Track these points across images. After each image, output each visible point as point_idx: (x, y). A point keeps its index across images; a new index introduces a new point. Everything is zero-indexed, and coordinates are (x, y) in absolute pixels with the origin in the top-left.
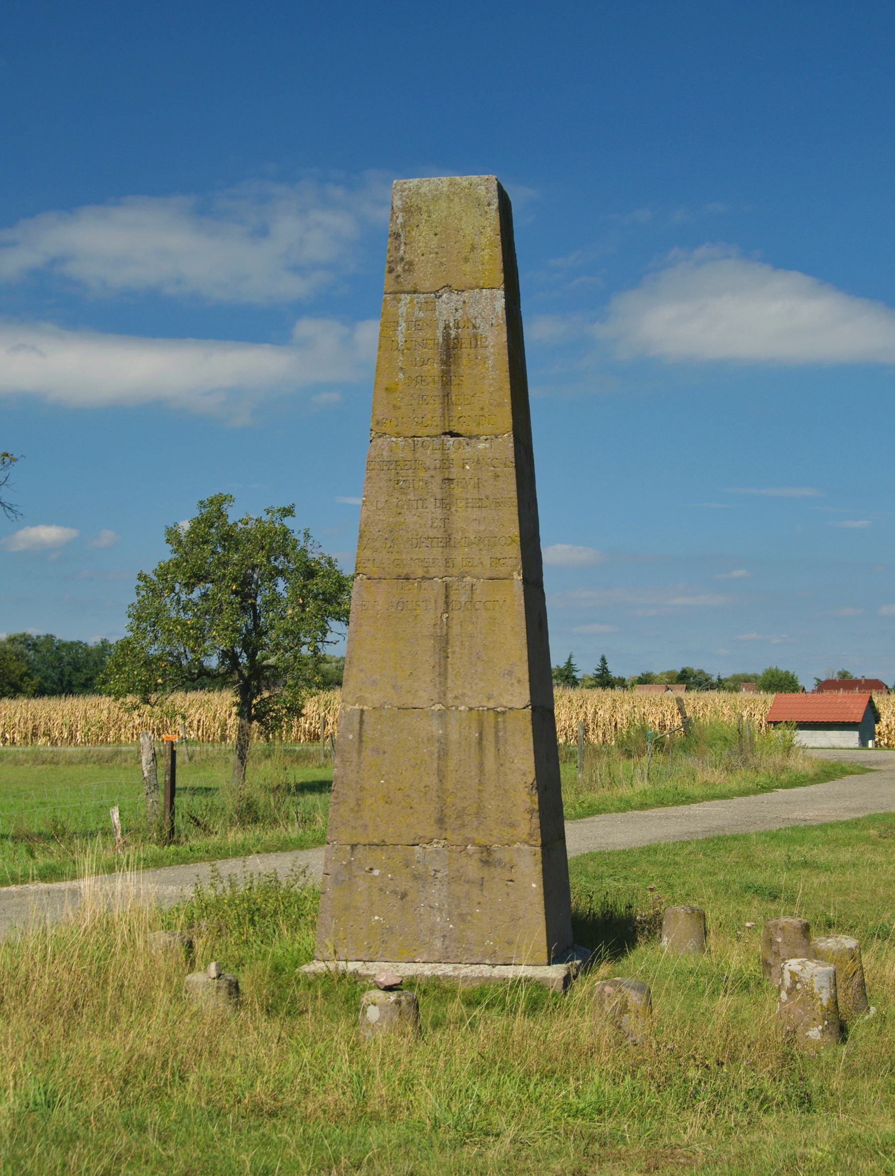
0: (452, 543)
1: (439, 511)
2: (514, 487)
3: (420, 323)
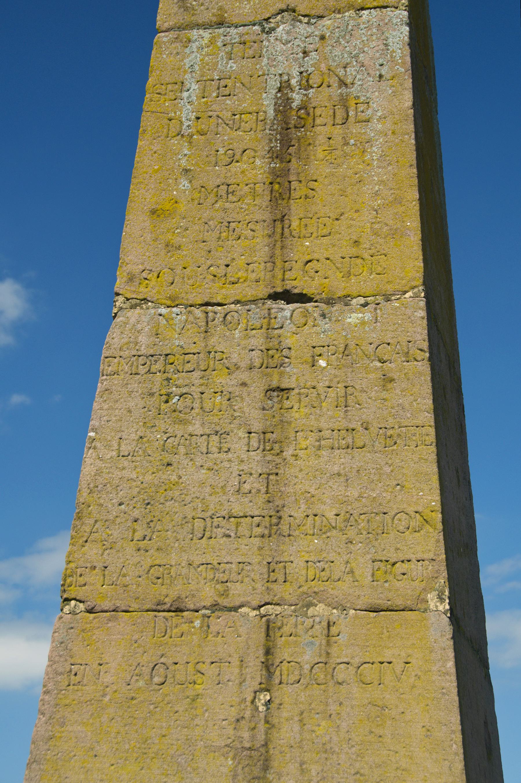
0: (284, 528)
1: (257, 456)
2: (429, 403)
3: (229, 83)
